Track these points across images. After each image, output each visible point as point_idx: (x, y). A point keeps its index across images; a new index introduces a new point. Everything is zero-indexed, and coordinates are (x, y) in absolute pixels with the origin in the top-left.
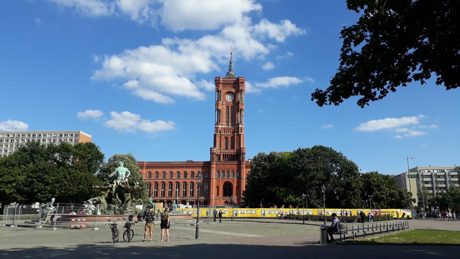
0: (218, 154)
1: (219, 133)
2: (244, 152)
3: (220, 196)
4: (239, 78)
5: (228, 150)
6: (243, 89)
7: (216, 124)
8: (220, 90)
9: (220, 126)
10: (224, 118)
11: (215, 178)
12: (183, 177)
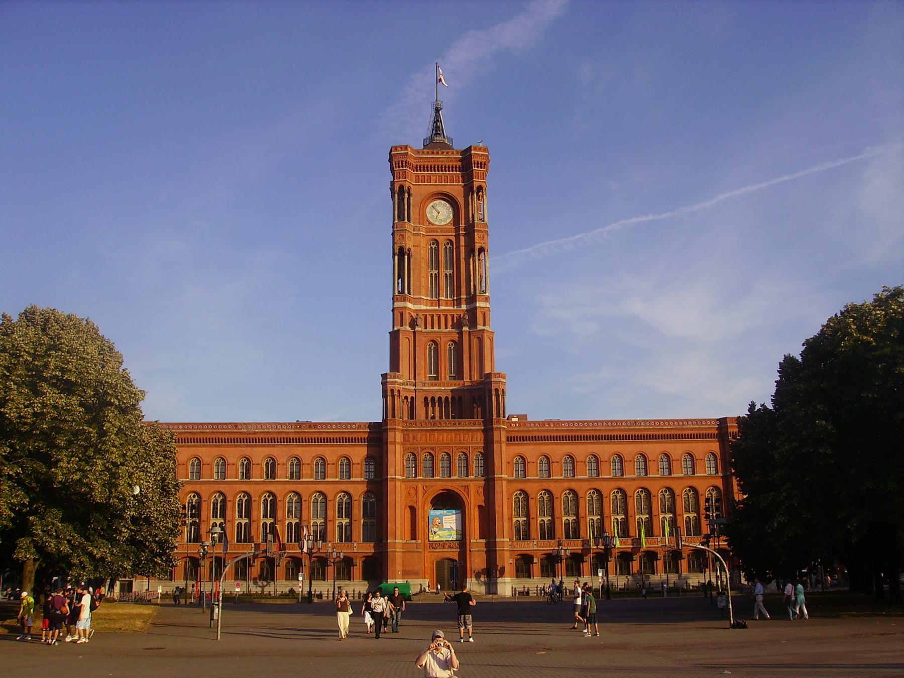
0: (406, 398)
2: (501, 387)
3: (419, 541)
5: (440, 385)
6: (483, 184)
7: (394, 299)
9: (409, 305)
10: (422, 279)
11: (403, 481)
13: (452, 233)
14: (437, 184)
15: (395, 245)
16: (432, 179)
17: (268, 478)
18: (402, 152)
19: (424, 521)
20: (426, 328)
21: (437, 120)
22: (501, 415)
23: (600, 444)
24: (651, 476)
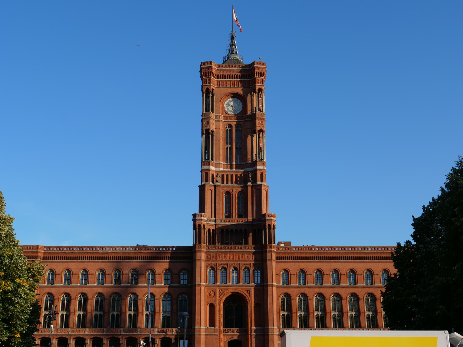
0: (209, 230)
1: (211, 183)
2: (273, 223)
4: (253, 63)
5: (232, 221)
6: (262, 87)
7: (203, 164)
8: (213, 90)
9: (212, 168)
10: (221, 151)
12: (129, 283)
13: (241, 119)
14: (232, 87)
15: (203, 128)
16: (228, 84)
17: (116, 283)
18: (208, 66)
19: (220, 314)
20: (223, 183)
21: (232, 45)
22: (272, 242)
23: (340, 262)
24: (376, 285)
